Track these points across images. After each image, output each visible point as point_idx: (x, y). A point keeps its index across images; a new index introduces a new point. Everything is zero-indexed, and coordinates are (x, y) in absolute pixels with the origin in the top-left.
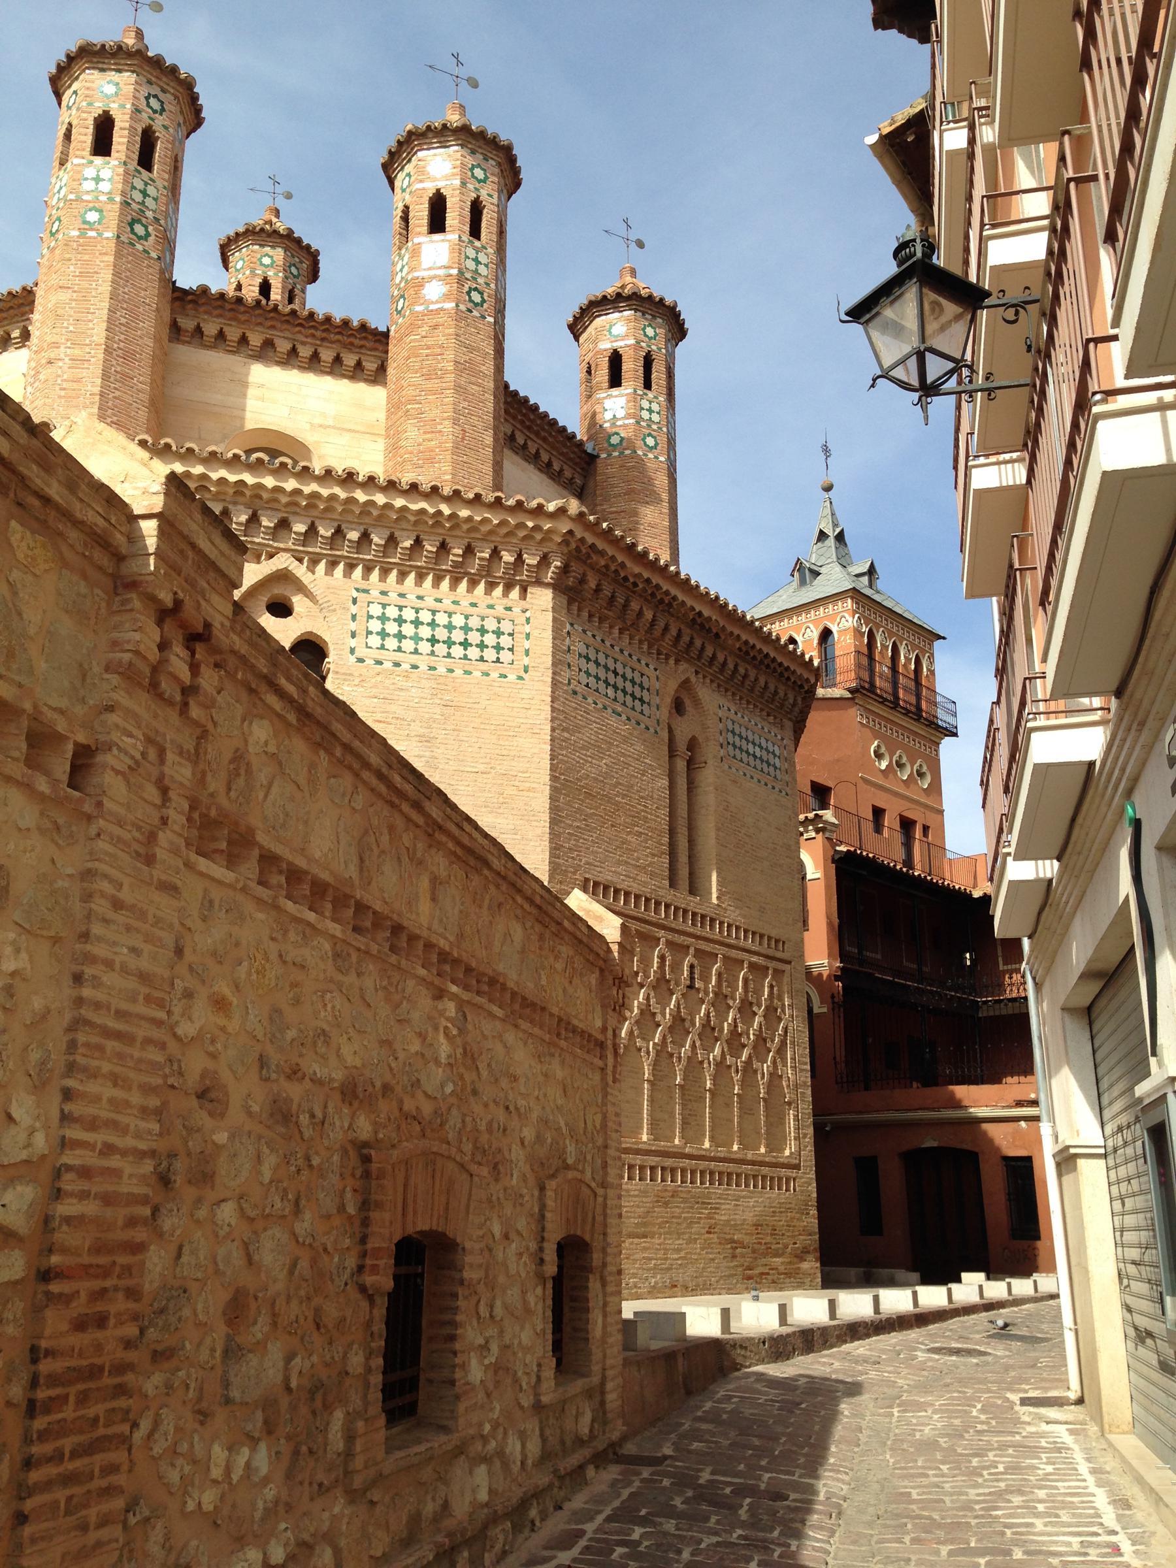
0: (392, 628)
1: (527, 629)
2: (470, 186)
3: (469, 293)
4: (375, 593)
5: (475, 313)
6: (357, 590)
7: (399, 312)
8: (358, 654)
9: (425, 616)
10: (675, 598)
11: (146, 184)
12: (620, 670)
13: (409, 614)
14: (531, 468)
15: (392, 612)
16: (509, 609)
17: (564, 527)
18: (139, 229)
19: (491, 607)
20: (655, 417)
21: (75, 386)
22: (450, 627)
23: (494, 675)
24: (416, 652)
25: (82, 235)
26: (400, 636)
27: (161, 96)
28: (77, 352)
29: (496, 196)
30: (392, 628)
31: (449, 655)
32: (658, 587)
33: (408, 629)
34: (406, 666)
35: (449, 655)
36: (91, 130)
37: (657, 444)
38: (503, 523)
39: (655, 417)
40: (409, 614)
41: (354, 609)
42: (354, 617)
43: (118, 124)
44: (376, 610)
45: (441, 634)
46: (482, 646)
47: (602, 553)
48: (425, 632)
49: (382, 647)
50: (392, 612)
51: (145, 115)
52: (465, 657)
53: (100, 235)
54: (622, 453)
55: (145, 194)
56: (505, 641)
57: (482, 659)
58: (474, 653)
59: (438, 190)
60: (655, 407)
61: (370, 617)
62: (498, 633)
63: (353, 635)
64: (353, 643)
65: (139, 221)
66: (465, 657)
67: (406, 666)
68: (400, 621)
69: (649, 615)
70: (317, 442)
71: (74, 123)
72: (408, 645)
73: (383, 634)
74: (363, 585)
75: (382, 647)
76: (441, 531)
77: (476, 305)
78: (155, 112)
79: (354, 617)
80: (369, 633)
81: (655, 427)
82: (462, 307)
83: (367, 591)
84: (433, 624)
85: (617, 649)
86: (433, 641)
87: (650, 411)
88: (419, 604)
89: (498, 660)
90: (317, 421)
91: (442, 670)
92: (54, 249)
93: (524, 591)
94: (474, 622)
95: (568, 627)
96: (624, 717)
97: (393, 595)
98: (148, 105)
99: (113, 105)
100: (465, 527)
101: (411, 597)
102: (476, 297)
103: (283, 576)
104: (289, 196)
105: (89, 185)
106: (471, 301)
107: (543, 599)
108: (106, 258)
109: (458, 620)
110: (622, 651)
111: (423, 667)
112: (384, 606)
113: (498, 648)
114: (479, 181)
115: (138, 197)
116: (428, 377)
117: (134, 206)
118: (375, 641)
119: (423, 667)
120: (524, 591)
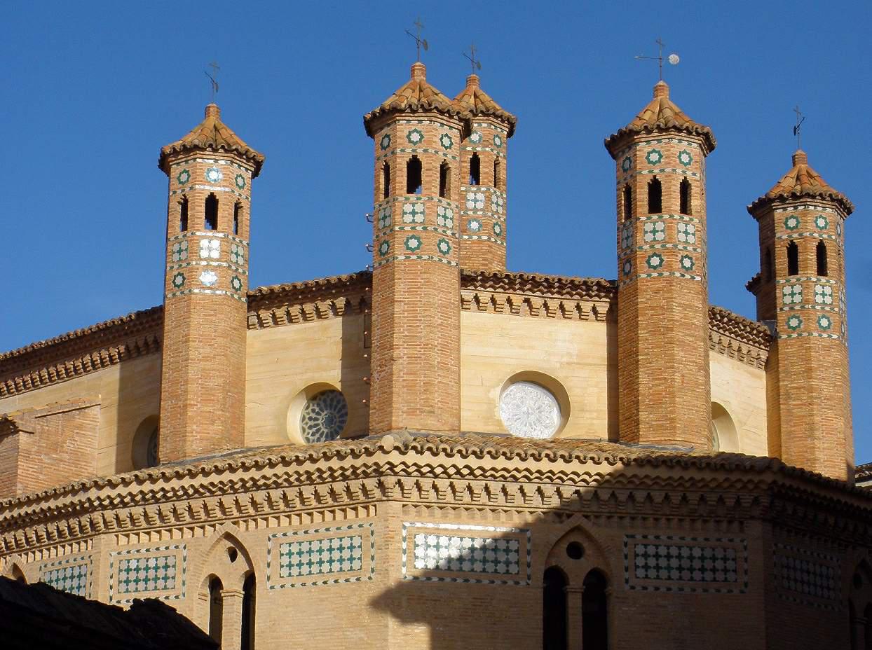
0: (652, 562)
1: (745, 554)
2: (679, 171)
3: (681, 261)
4: (639, 537)
5: (688, 276)
6: (627, 536)
7: (627, 274)
8: (631, 583)
9: (674, 551)
10: (852, 505)
11: (445, 209)
12: (812, 570)
13: (662, 551)
14: (725, 358)
15: (651, 550)
16: (731, 540)
17: (768, 478)
19: (719, 540)
20: (828, 300)
21: (411, 377)
22: (691, 558)
23: (724, 591)
24: (669, 578)
25: (407, 258)
26: (658, 568)
27: (450, 133)
28: (411, 351)
29: (698, 175)
30: (652, 562)
31: (692, 579)
32: (839, 501)
33: (663, 562)
34: (663, 589)
35: (692, 579)
37: (830, 324)
38: (727, 480)
39: (828, 300)
40: (662, 551)
41: (625, 550)
42: (626, 557)
43: (424, 165)
44: (640, 550)
45: (686, 563)
46: (714, 570)
47: (798, 489)
48: (674, 563)
49: (647, 577)
50: (651, 550)
51: (441, 153)
52: (703, 579)
53: (419, 258)
54: (800, 335)
55: (445, 217)
56: (730, 565)
57: (715, 580)
58: (709, 576)
59: (655, 177)
60: (828, 290)
61: (636, 555)
62: (725, 559)
63: (627, 569)
64: (627, 575)
65: (443, 240)
66: (703, 579)
67: (663, 589)
68: (657, 556)
69: (831, 521)
70: (566, 377)
72: (664, 574)
73: (646, 567)
74: (630, 532)
75: (647, 577)
76: (681, 489)
77: (687, 269)
78: (446, 148)
79: (626, 557)
80: (637, 567)
81: (827, 309)
82: (677, 274)
83: (633, 536)
84: (679, 557)
85: (809, 553)
86: (680, 569)
87: (823, 295)
88: (670, 542)
89: (726, 580)
90: (565, 359)
91: (687, 590)
93: (741, 523)
94: (708, 553)
95: (774, 548)
96: (816, 605)
97: (651, 537)
98: (443, 145)
99: (420, 151)
100: (700, 485)
101: (663, 537)
102: (687, 263)
103: (578, 529)
105: (408, 218)
106: (683, 267)
107: (756, 529)
109: (697, 552)
110: (812, 554)
111: (675, 588)
112: (646, 546)
113: (725, 570)
114: (686, 164)
115: (441, 221)
116: (653, 333)
117: (440, 230)
118: (641, 572)
119: (675, 588)
120: (741, 523)
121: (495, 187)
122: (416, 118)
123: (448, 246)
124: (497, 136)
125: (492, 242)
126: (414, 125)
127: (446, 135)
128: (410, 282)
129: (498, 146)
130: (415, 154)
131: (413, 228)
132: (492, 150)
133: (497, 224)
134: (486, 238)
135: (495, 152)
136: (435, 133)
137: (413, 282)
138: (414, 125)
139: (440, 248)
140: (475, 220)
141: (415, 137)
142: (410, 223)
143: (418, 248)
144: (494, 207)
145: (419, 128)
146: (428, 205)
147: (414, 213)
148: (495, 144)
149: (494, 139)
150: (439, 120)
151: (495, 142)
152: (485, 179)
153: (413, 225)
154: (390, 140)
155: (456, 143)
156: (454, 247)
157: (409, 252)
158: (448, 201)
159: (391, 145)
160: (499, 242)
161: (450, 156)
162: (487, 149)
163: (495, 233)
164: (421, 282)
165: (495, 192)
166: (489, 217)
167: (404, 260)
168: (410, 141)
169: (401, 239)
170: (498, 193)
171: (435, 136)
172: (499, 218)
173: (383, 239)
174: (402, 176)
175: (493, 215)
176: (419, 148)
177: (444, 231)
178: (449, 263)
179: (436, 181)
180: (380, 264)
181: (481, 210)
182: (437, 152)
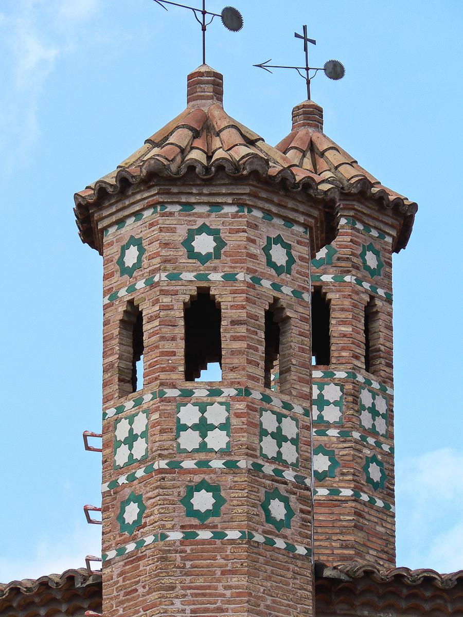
11: (280, 417)
18: (278, 509)
25: (189, 537)
36: (180, 331)
51: (266, 284)
55: (279, 437)
71: (147, 310)
78: (279, 270)
92: (134, 559)
99: (216, 277)
104: (335, 71)
105: (190, 440)
108: (234, 580)
115: (269, 446)
117: (268, 469)
121: (367, 370)
122: (205, 199)
123: (287, 507)
124: (371, 248)
125: (364, 504)
126: (200, 216)
127: (279, 240)
128: (196, 595)
129: (373, 272)
130: (204, 284)
131: (203, 465)
132: (359, 282)
133: (373, 459)
134: (347, 492)
135: (366, 285)
136: (252, 233)
137: (204, 595)
138: (200, 216)
139: (268, 512)
140: (321, 449)
141: (204, 244)
142: (195, 451)
143: (215, 511)
144: (366, 419)
145: (213, 221)
146: (241, 406)
147: (203, 427)
148: (367, 268)
149: (363, 255)
150: (261, 204)
151: (365, 262)
152: (343, 349)
153: (202, 456)
154: (141, 250)
155: (302, 259)
156: (302, 511)
157: (195, 521)
158: (286, 398)
159: (145, 262)
160: (380, 503)
161: (287, 290)
162: (348, 278)
163: (369, 480)
164: (224, 595)
165: (368, 382)
166: (356, 442)
167: (182, 543)
168: (192, 254)
169: (175, 491)
170: (376, 385)
171: (253, 241)
172: (379, 444)
173: (128, 491)
174: (173, 339)
175: (363, 438)
176: (215, 269)
177: (278, 472)
178: (290, 548)
179: (256, 350)
180: (121, 552)
181: (336, 425)
182: (256, 280)
